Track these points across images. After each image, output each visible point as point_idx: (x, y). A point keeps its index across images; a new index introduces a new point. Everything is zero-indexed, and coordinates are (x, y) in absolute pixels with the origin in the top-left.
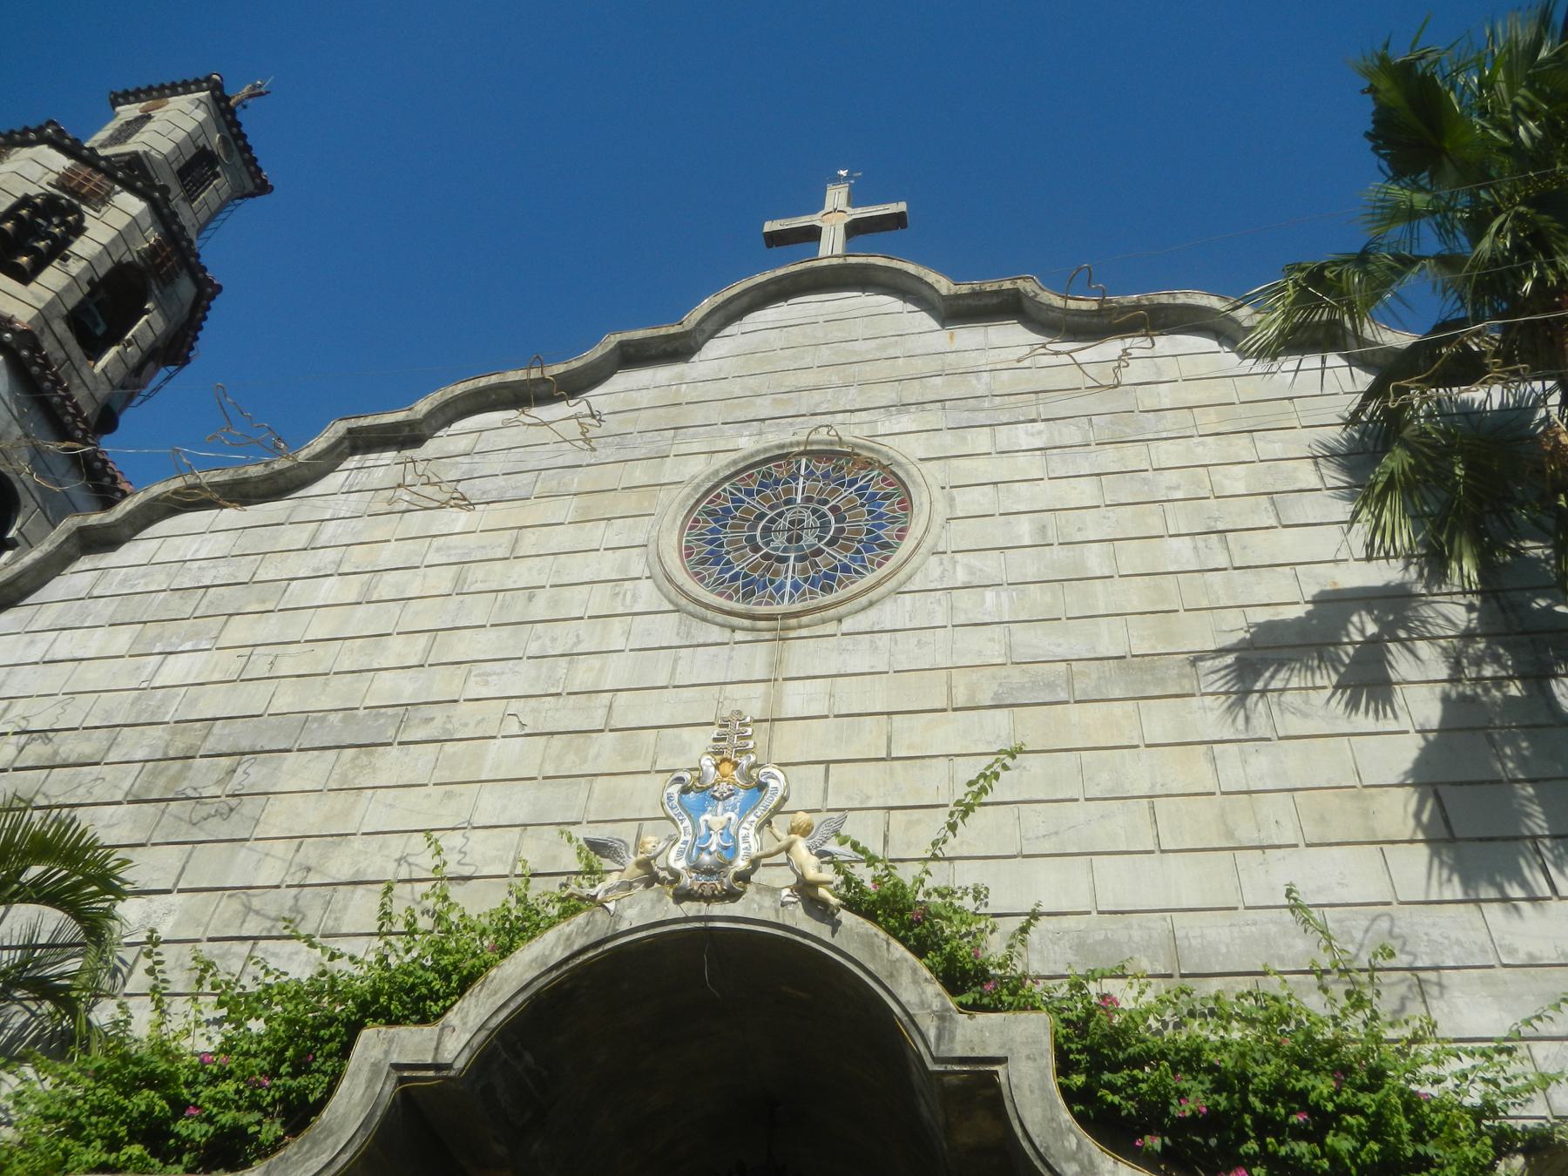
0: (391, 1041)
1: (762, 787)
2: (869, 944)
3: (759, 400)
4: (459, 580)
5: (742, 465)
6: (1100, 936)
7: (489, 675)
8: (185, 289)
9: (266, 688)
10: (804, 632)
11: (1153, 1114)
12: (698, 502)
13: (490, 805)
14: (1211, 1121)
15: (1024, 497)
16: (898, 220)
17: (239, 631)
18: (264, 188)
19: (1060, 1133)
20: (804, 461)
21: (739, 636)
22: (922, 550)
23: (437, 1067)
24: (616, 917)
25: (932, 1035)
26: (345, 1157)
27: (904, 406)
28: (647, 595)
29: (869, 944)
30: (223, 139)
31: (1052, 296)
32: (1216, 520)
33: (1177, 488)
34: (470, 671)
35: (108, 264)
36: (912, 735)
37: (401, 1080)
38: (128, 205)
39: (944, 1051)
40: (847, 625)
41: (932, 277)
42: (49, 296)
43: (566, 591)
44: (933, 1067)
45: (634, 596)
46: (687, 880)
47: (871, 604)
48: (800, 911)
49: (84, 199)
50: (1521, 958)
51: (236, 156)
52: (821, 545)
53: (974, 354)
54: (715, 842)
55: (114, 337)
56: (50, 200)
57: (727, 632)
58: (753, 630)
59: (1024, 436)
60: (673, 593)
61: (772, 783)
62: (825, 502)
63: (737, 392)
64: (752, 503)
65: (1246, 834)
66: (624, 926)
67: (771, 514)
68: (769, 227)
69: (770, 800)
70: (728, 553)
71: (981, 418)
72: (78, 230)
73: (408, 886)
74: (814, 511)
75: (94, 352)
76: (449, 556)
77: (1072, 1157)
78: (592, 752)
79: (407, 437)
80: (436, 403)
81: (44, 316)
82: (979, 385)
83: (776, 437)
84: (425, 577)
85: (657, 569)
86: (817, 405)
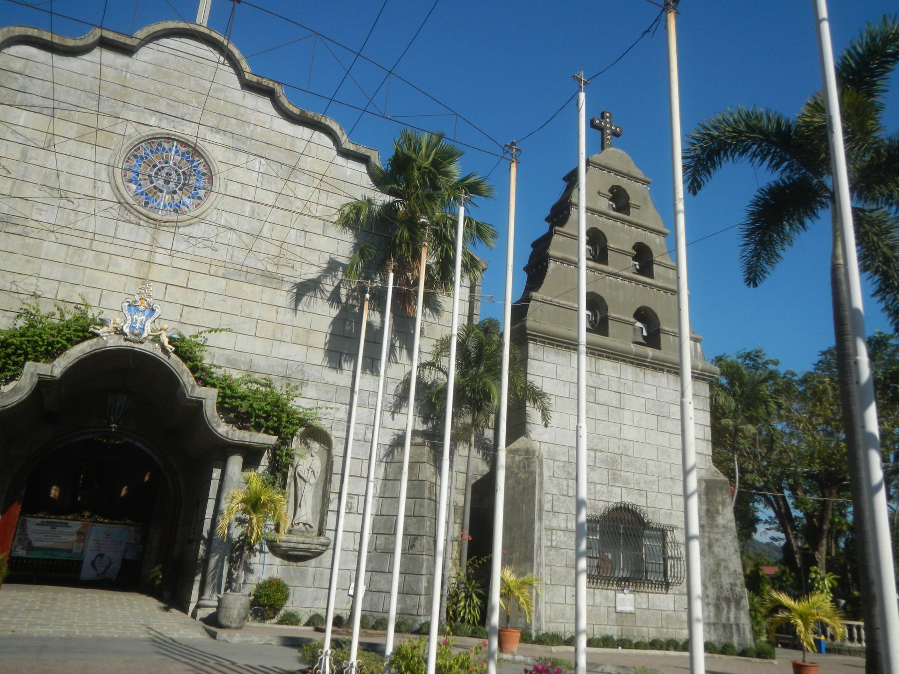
0: (36, 367)
1: (153, 310)
2: (177, 364)
3: (161, 100)
4: (24, 154)
5: (150, 137)
6: (233, 357)
7: (41, 210)
10: (165, 229)
11: (234, 409)
12: (131, 149)
13: (45, 269)
14: (247, 413)
15: (250, 194)
19: (214, 417)
20: (175, 143)
21: (142, 223)
22: (212, 207)
23: (51, 376)
24: (106, 342)
25: (189, 390)
26: (25, 397)
27: (218, 130)
28: (107, 192)
29: (177, 364)
31: (285, 100)
32: (306, 226)
33: (298, 208)
34: (33, 206)
36: (197, 281)
37: (39, 378)
39: (192, 395)
40: (181, 230)
41: (244, 65)
43: (74, 179)
44: (188, 397)
45: (102, 190)
46: (130, 336)
47: (191, 224)
48: (160, 351)
50: (325, 381)
52: (177, 189)
53: (250, 112)
54: (138, 325)
57: (138, 219)
58: (147, 222)
59: (256, 163)
60: (118, 195)
61: (157, 310)
62: (181, 168)
63: (152, 91)
64: (152, 157)
65: (278, 336)
66: (108, 345)
67: (159, 166)
69: (156, 315)
70: (140, 180)
71: (245, 148)
73: (16, 295)
74: (176, 171)
76: (18, 138)
77: (215, 423)
78: (85, 258)
80: (6, 37)
82: (248, 130)
83: (167, 127)
84: (7, 147)
85: (113, 181)
86: (186, 114)
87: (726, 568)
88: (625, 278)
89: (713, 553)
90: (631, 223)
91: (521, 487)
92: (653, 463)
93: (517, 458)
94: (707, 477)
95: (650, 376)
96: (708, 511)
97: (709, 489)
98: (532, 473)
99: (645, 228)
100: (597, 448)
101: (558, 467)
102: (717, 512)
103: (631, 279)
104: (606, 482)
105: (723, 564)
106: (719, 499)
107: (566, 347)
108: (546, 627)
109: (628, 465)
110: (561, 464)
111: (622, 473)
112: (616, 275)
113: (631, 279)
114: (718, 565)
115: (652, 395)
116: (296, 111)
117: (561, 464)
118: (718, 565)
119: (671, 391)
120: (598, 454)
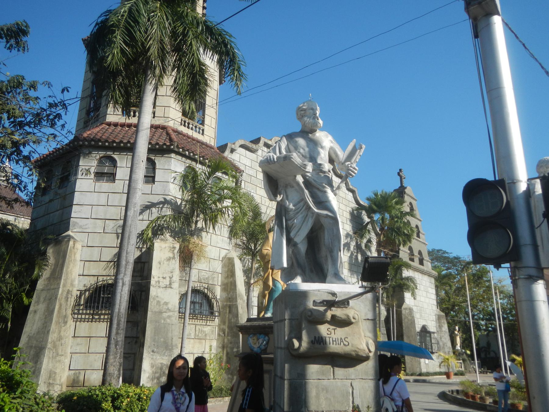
87: (446, 346)
89: (442, 341)
91: (410, 322)
93: (407, 311)
94: (438, 314)
96: (439, 326)
97: (439, 318)
98: (413, 317)
102: (442, 326)
105: (445, 344)
106: (442, 321)
108: (424, 370)
114: (444, 345)
115: (424, 285)
116: (339, 173)
118: (444, 345)
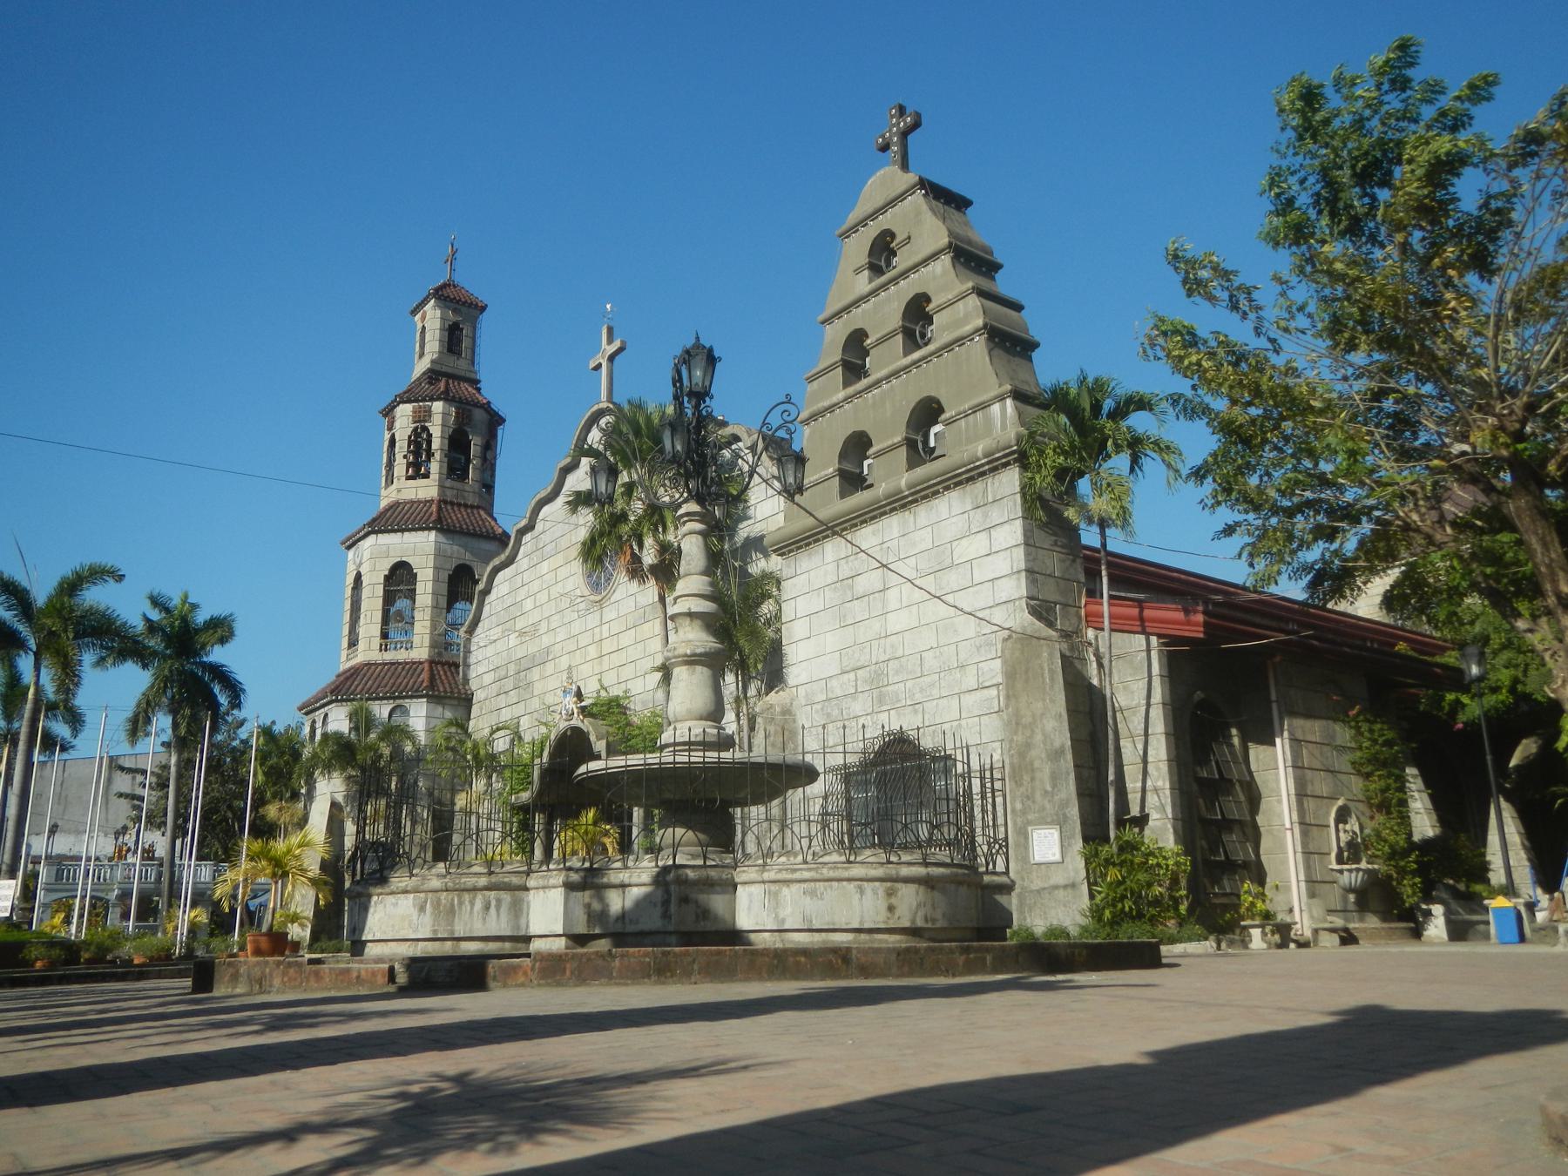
8: (479, 415)
9: (524, 646)
16: (621, 350)
17: (520, 624)
18: (483, 309)
30: (454, 311)
35: (446, 442)
38: (438, 406)
40: (612, 600)
42: (437, 476)
49: (425, 421)
51: (464, 309)
55: (468, 461)
56: (415, 430)
68: (592, 365)
72: (430, 435)
75: (464, 476)
79: (530, 527)
81: (441, 487)
88: (888, 378)
90: (894, 280)
92: (931, 653)
95: (924, 514)
99: (915, 268)
100: (859, 664)
101: (817, 712)
103: (895, 374)
104: (870, 711)
107: (815, 541)
109: (897, 672)
110: (819, 707)
111: (889, 688)
112: (877, 383)
113: (895, 374)
117: (819, 707)
119: (954, 520)
120: (860, 672)
